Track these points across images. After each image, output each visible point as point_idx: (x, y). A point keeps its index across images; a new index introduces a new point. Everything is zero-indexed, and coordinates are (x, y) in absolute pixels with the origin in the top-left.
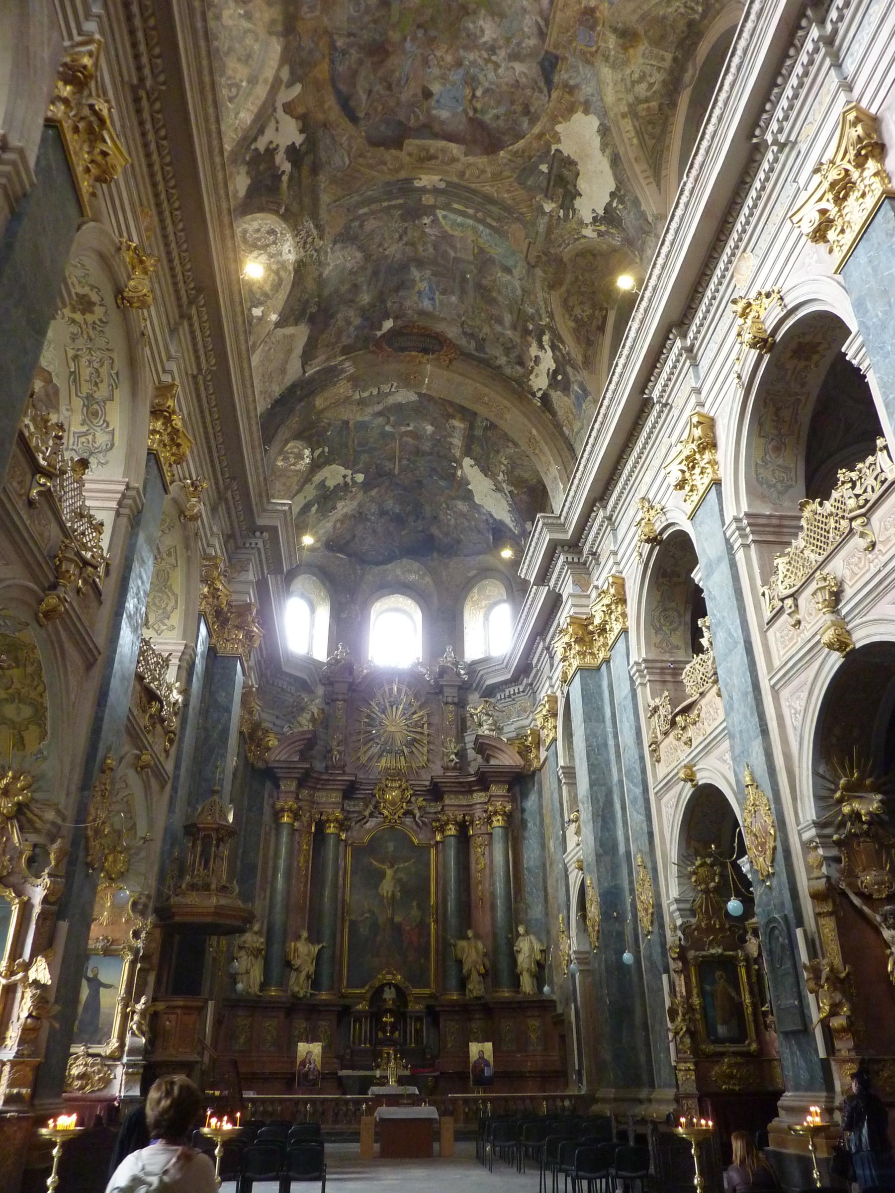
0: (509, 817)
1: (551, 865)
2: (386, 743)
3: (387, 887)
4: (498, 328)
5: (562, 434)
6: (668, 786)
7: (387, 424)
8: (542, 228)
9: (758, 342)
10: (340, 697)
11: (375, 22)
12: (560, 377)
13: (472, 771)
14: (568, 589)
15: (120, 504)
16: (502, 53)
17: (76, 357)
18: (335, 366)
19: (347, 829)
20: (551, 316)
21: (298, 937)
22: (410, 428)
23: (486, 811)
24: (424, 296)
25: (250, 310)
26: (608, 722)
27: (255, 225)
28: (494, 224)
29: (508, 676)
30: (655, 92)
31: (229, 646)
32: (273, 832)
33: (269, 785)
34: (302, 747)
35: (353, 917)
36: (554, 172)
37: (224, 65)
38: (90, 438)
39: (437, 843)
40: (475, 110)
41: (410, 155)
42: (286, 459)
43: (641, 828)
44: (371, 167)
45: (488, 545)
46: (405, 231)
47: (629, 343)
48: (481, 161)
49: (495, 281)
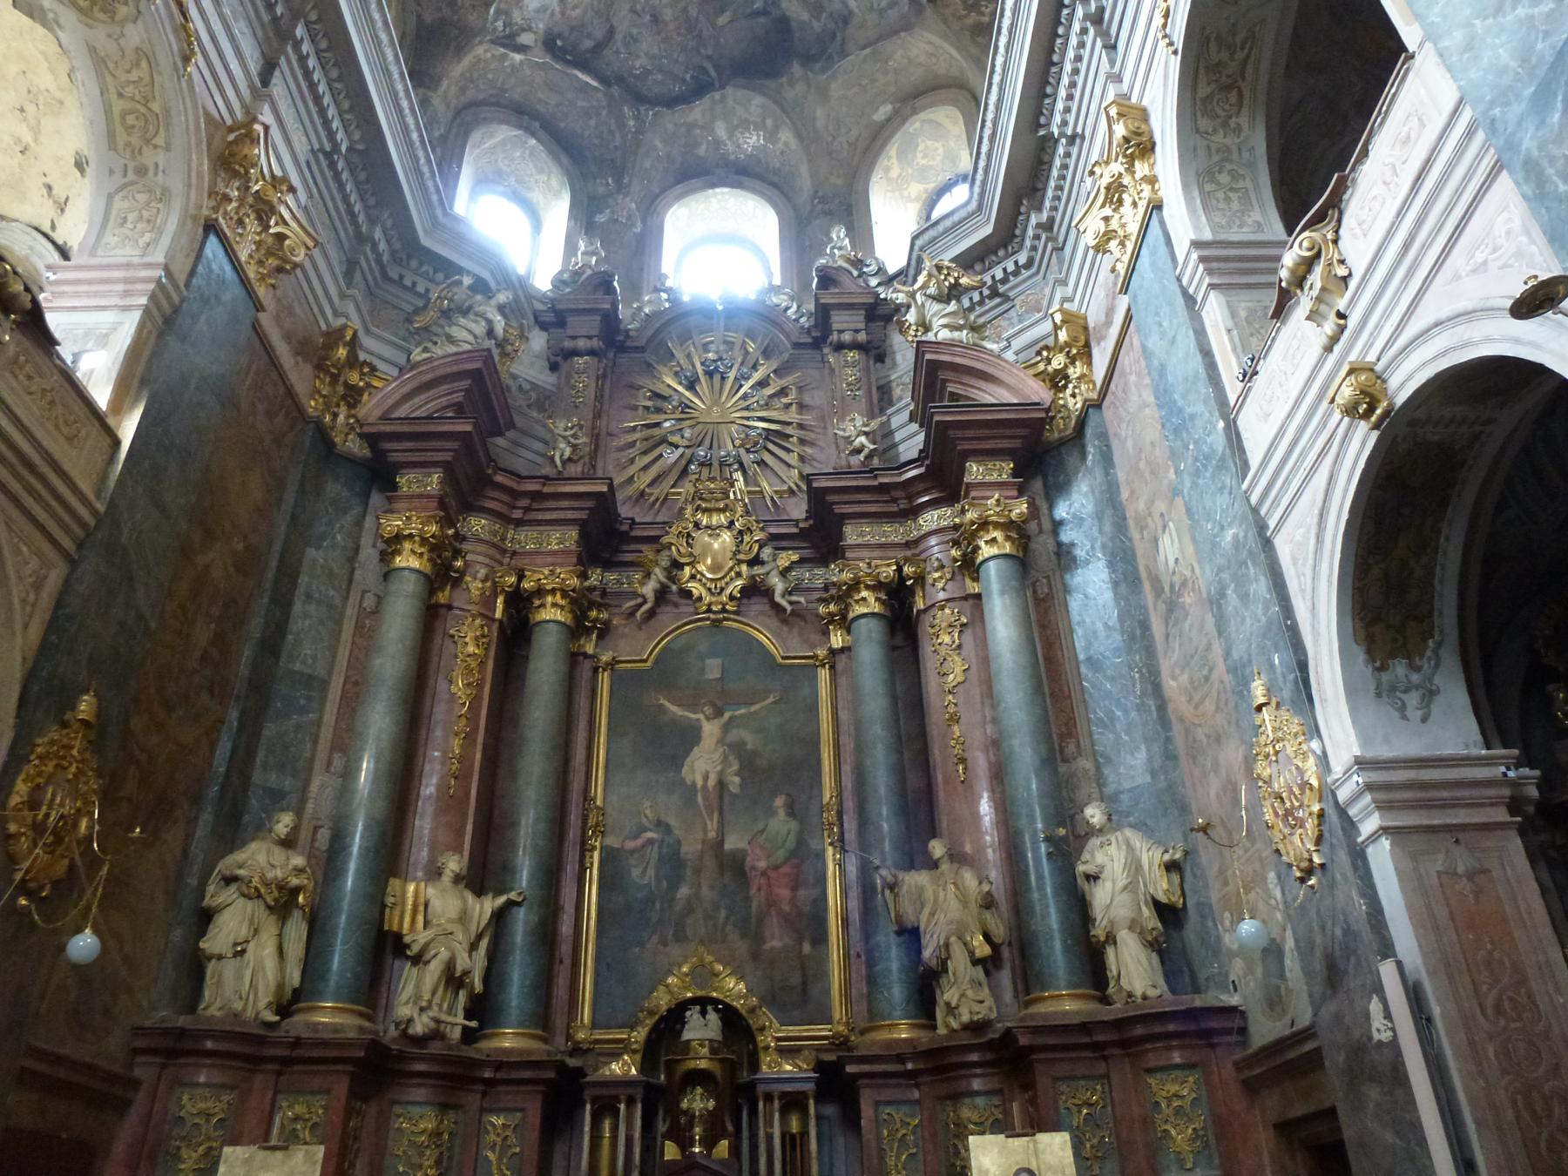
1: (1172, 607)
3: (704, 764)
10: (582, 344)
29: (988, 230)
34: (458, 397)
35: (612, 841)
39: (833, 652)
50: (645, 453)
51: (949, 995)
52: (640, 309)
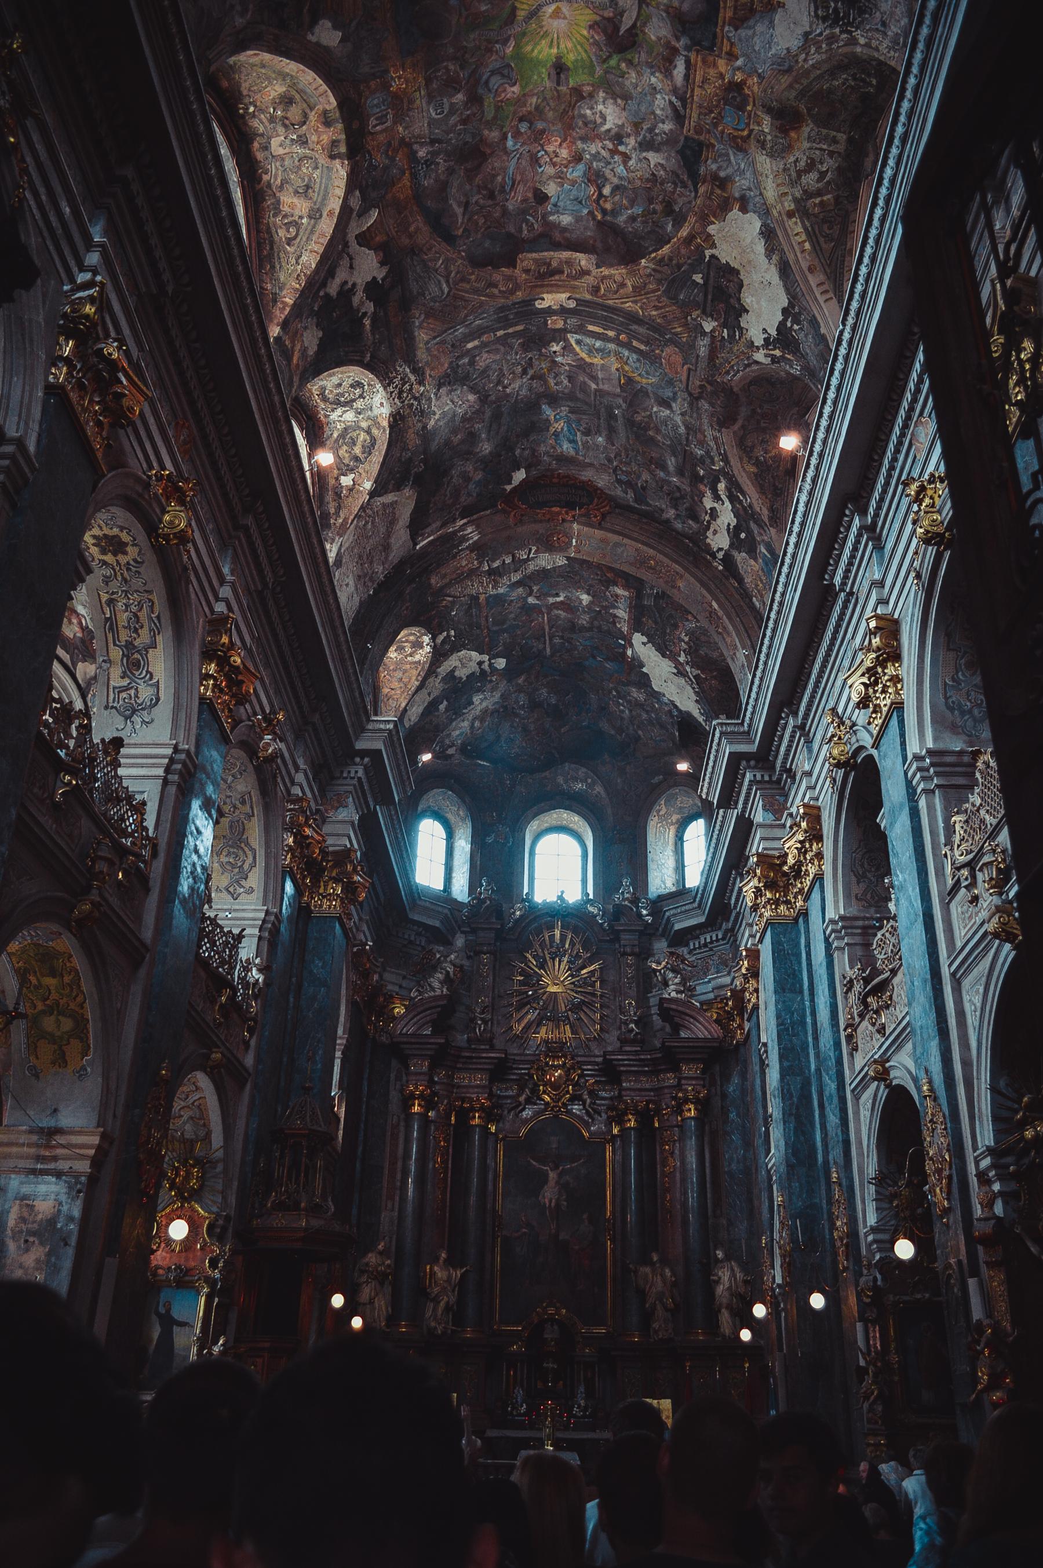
0: (703, 1106)
2: (544, 1008)
3: (549, 1194)
4: (662, 474)
5: (752, 607)
6: (863, 1085)
7: (530, 595)
8: (703, 351)
9: (932, 538)
11: (464, 122)
12: (743, 536)
13: (658, 1044)
14: (759, 816)
15: (168, 770)
16: (632, 142)
17: (111, 602)
18: (455, 533)
19: (497, 1119)
20: (726, 459)
21: (435, 1260)
22: (561, 599)
23: (675, 1098)
24: (563, 434)
25: (337, 479)
26: (806, 992)
27: (335, 380)
28: (643, 347)
29: (702, 919)
30: (829, 183)
31: (326, 904)
32: (402, 1124)
33: (394, 1063)
34: (435, 1016)
36: (711, 282)
37: (278, 202)
38: (132, 692)
39: (614, 1136)
40: (604, 212)
41: (527, 271)
42: (401, 649)
43: (836, 1134)
44: (476, 291)
45: (674, 743)
46: (530, 363)
47: (798, 519)
48: (618, 272)
49: (650, 416)
50: (519, 1009)
51: (656, 1325)
52: (514, 913)
